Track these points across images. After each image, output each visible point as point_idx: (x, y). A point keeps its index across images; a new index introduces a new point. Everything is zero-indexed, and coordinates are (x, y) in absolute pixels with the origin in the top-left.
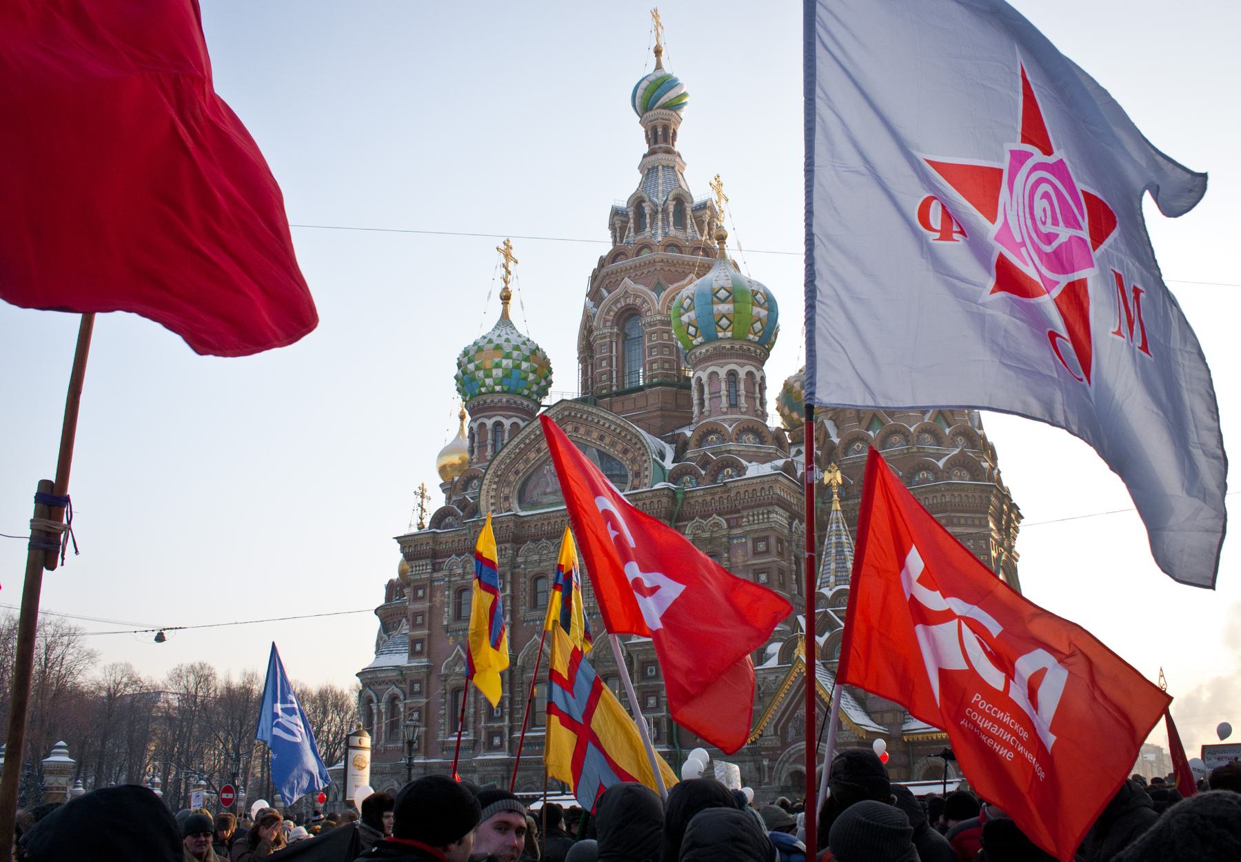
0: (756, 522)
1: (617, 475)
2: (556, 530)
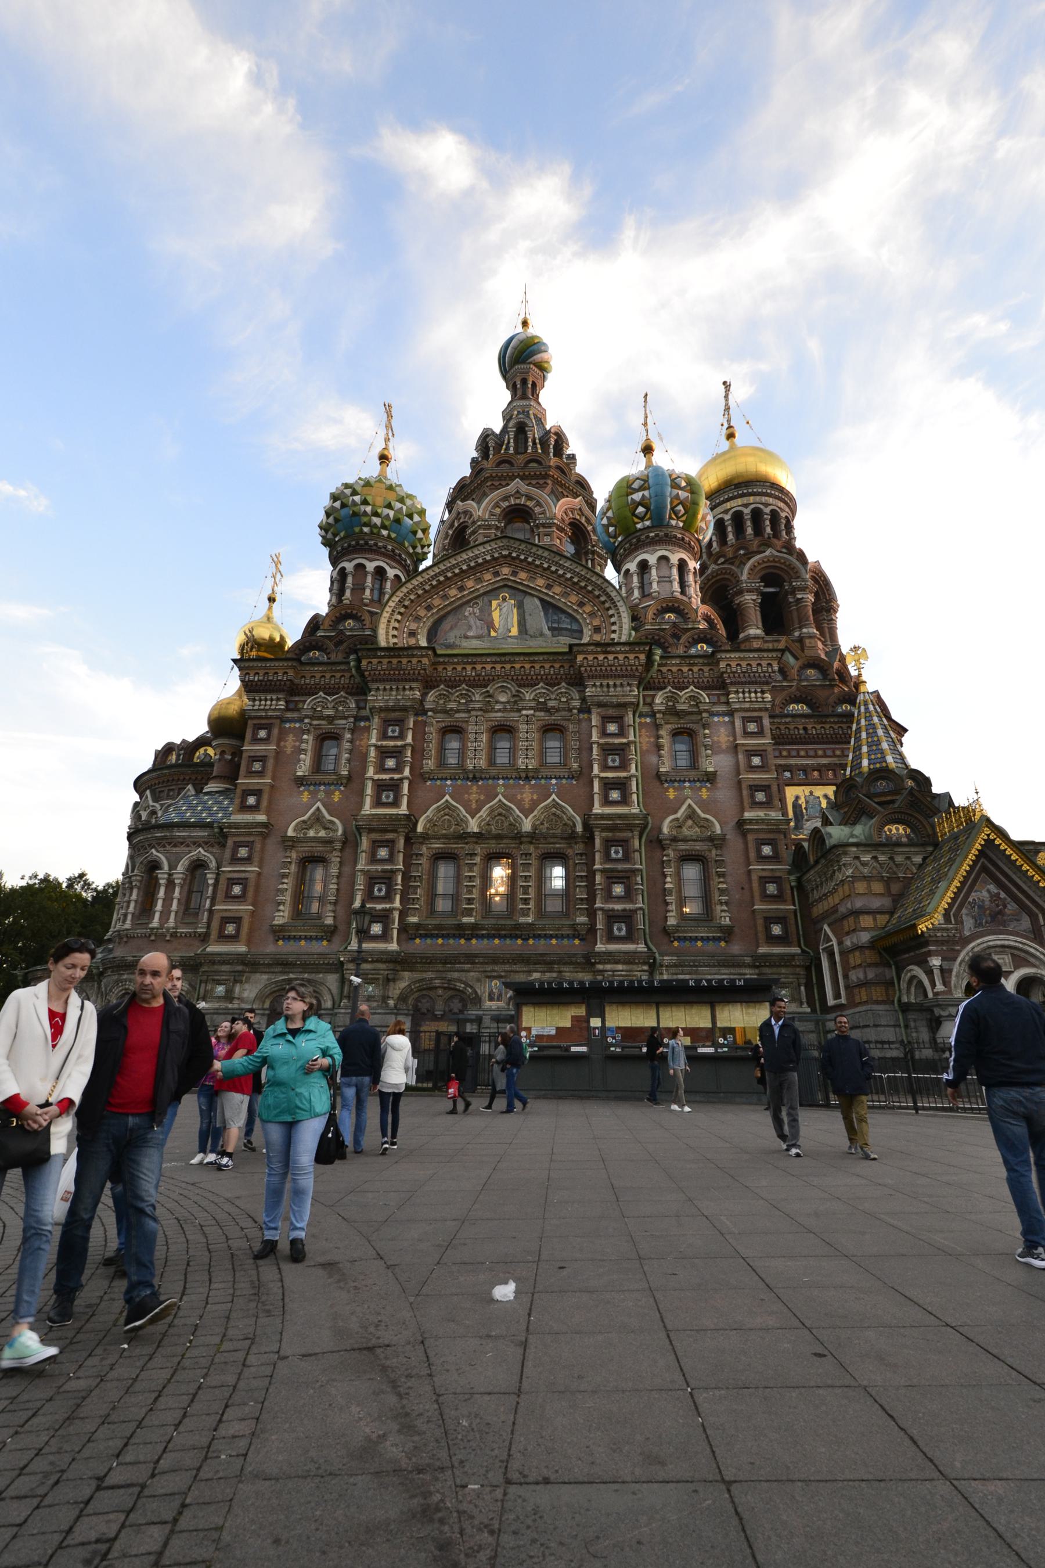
0: (747, 700)
1: (566, 629)
2: (481, 678)
